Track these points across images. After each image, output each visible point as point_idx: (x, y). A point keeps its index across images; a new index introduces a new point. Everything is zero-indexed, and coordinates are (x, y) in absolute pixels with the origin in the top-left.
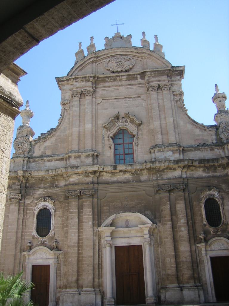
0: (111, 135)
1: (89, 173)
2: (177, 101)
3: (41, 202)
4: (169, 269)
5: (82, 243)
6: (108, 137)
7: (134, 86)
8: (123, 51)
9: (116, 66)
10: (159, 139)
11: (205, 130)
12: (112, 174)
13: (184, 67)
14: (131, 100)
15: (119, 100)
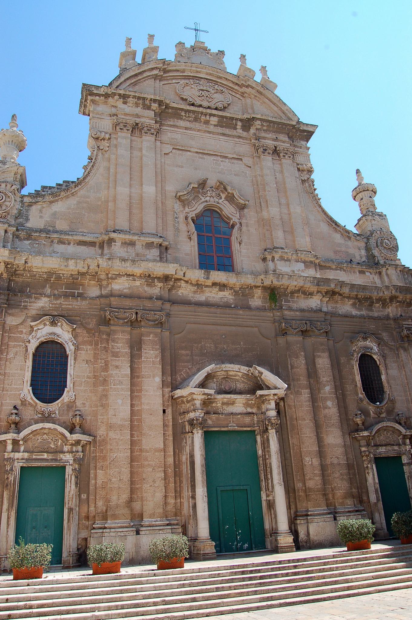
0: (193, 214)
2: (303, 181)
3: (45, 325)
4: (310, 479)
5: (140, 420)
6: (186, 218)
7: (231, 139)
8: (211, 74)
9: (199, 96)
11: (349, 238)
12: (198, 288)
13: (316, 127)
14: (225, 162)
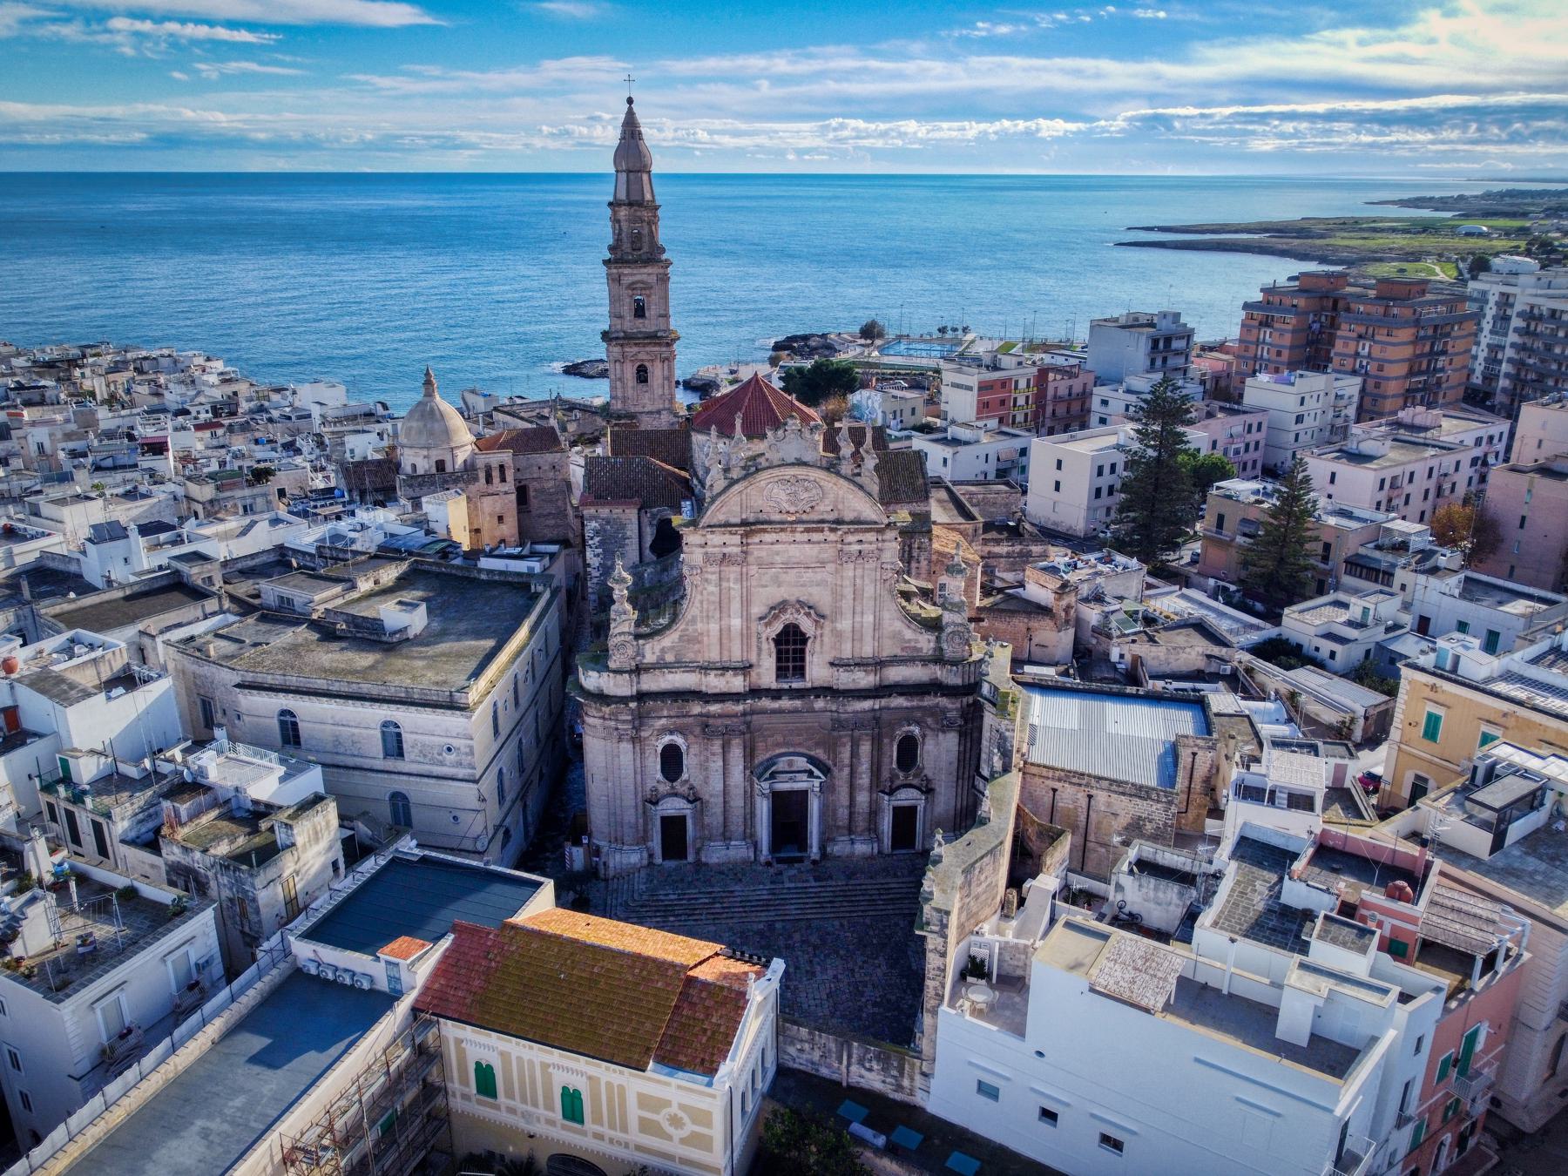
10: (846, 652)
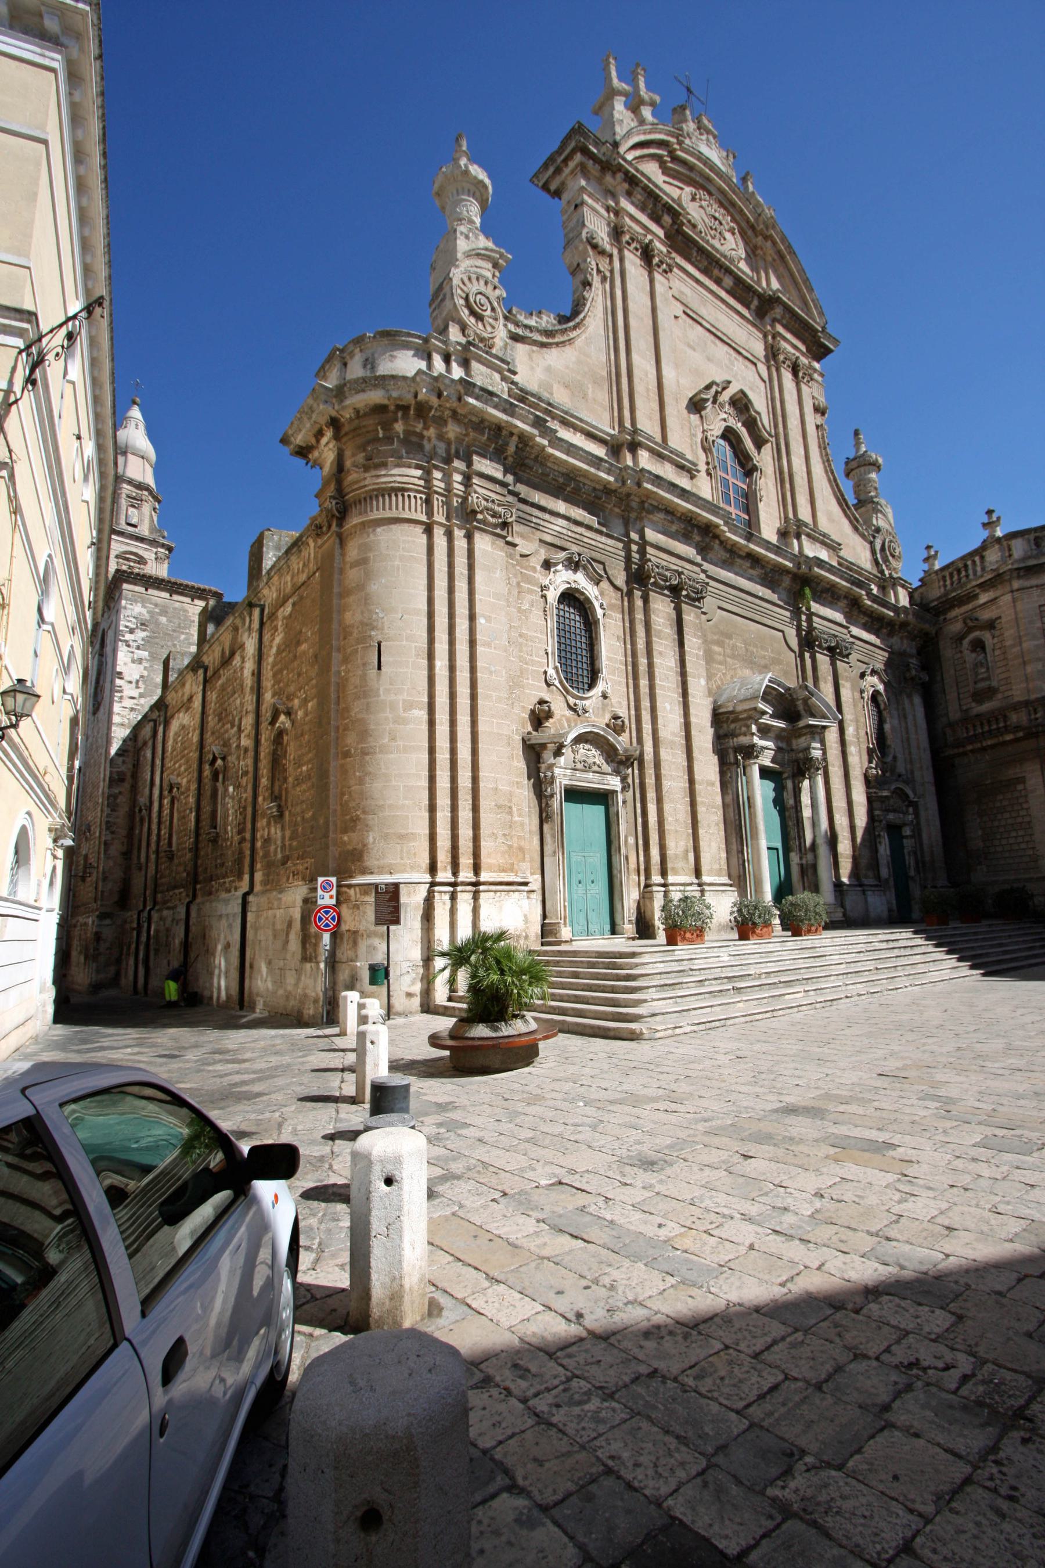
1: (694, 526)
15: (717, 342)
